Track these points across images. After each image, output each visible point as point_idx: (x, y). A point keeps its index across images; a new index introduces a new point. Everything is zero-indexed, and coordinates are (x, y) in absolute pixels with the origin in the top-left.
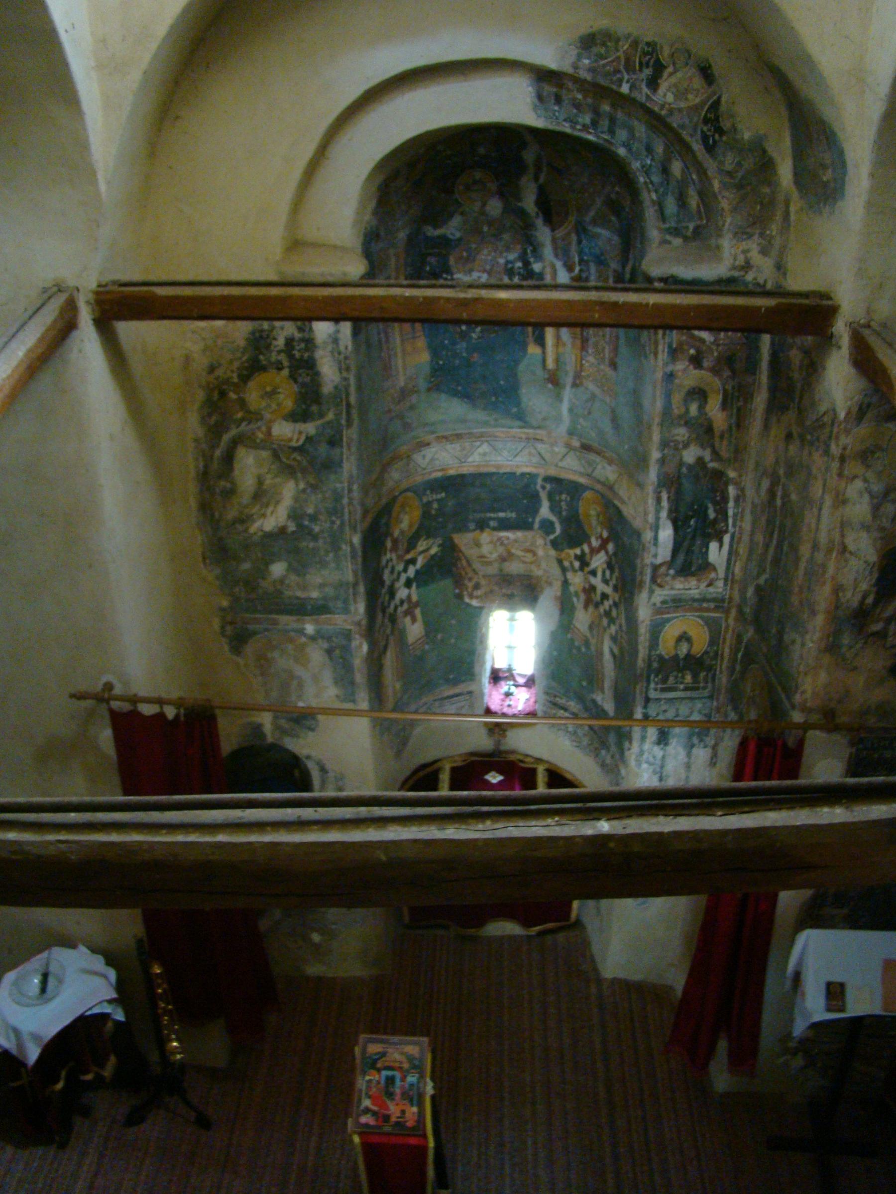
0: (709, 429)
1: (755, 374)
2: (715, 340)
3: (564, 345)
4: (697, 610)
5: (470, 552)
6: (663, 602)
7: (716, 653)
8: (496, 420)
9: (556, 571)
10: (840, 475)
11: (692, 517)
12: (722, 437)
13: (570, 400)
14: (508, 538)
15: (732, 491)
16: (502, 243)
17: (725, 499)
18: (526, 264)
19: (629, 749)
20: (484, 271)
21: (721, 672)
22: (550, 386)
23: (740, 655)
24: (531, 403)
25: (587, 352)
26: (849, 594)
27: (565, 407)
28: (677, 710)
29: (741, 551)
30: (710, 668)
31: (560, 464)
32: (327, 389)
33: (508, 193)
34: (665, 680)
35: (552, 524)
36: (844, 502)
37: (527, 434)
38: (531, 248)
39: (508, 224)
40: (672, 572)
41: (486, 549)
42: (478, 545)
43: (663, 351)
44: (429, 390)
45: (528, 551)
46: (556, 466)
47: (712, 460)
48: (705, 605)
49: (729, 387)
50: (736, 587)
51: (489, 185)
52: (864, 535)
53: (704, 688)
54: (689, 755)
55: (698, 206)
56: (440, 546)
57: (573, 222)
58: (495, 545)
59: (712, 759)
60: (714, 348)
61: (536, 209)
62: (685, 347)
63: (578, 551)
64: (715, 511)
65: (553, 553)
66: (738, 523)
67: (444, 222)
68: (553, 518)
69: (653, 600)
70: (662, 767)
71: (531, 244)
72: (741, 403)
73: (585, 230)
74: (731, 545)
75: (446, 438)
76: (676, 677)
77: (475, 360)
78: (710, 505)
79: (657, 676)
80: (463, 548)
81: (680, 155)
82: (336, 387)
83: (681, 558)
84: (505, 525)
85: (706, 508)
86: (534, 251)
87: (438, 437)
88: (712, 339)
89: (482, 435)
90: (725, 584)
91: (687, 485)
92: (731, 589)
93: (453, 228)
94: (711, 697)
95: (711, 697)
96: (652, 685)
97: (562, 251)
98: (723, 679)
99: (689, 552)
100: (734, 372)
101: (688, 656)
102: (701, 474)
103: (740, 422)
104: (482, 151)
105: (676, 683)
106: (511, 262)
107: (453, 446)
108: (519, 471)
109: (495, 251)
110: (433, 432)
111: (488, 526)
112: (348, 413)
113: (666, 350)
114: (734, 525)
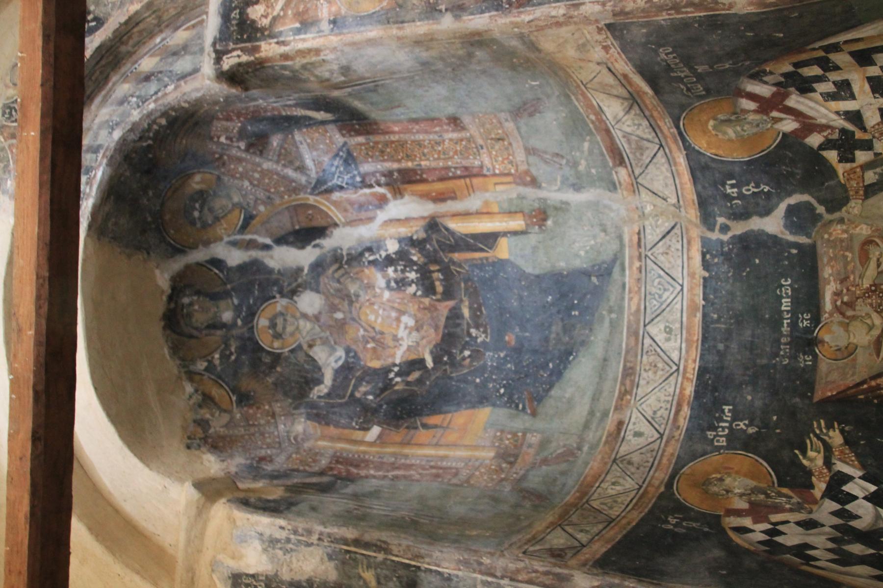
3: (486, 203)
5: (864, 364)
8: (610, 311)
13: (559, 190)
14: (837, 294)
16: (361, 293)
18: (389, 261)
20: (398, 320)
22: (549, 223)
24: (582, 253)
25: (481, 167)
31: (673, 200)
32: (330, 572)
33: (290, 284)
35: (791, 211)
37: (631, 258)
39: (337, 285)
41: (861, 337)
42: (850, 351)
43: (304, 40)
44: (534, 414)
45: (864, 258)
46: (678, 206)
51: (279, 308)
55: (187, 29)
56: (830, 426)
57: (318, 198)
58: (854, 318)
61: (309, 248)
63: (832, 156)
65: (855, 207)
67: (320, 369)
68: (783, 207)
71: (361, 254)
73: (320, 182)
75: (621, 397)
77: (513, 337)
80: (850, 381)
81: (136, 62)
82: (330, 557)
84: (809, 299)
86: (370, 249)
87: (616, 409)
89: (634, 333)
93: (329, 360)
97: (362, 213)
104: (227, 316)
106: (388, 283)
107: (642, 382)
108: (701, 273)
109: (373, 304)
110: (605, 414)
111: (809, 330)
112: (367, 545)
113: (302, 36)
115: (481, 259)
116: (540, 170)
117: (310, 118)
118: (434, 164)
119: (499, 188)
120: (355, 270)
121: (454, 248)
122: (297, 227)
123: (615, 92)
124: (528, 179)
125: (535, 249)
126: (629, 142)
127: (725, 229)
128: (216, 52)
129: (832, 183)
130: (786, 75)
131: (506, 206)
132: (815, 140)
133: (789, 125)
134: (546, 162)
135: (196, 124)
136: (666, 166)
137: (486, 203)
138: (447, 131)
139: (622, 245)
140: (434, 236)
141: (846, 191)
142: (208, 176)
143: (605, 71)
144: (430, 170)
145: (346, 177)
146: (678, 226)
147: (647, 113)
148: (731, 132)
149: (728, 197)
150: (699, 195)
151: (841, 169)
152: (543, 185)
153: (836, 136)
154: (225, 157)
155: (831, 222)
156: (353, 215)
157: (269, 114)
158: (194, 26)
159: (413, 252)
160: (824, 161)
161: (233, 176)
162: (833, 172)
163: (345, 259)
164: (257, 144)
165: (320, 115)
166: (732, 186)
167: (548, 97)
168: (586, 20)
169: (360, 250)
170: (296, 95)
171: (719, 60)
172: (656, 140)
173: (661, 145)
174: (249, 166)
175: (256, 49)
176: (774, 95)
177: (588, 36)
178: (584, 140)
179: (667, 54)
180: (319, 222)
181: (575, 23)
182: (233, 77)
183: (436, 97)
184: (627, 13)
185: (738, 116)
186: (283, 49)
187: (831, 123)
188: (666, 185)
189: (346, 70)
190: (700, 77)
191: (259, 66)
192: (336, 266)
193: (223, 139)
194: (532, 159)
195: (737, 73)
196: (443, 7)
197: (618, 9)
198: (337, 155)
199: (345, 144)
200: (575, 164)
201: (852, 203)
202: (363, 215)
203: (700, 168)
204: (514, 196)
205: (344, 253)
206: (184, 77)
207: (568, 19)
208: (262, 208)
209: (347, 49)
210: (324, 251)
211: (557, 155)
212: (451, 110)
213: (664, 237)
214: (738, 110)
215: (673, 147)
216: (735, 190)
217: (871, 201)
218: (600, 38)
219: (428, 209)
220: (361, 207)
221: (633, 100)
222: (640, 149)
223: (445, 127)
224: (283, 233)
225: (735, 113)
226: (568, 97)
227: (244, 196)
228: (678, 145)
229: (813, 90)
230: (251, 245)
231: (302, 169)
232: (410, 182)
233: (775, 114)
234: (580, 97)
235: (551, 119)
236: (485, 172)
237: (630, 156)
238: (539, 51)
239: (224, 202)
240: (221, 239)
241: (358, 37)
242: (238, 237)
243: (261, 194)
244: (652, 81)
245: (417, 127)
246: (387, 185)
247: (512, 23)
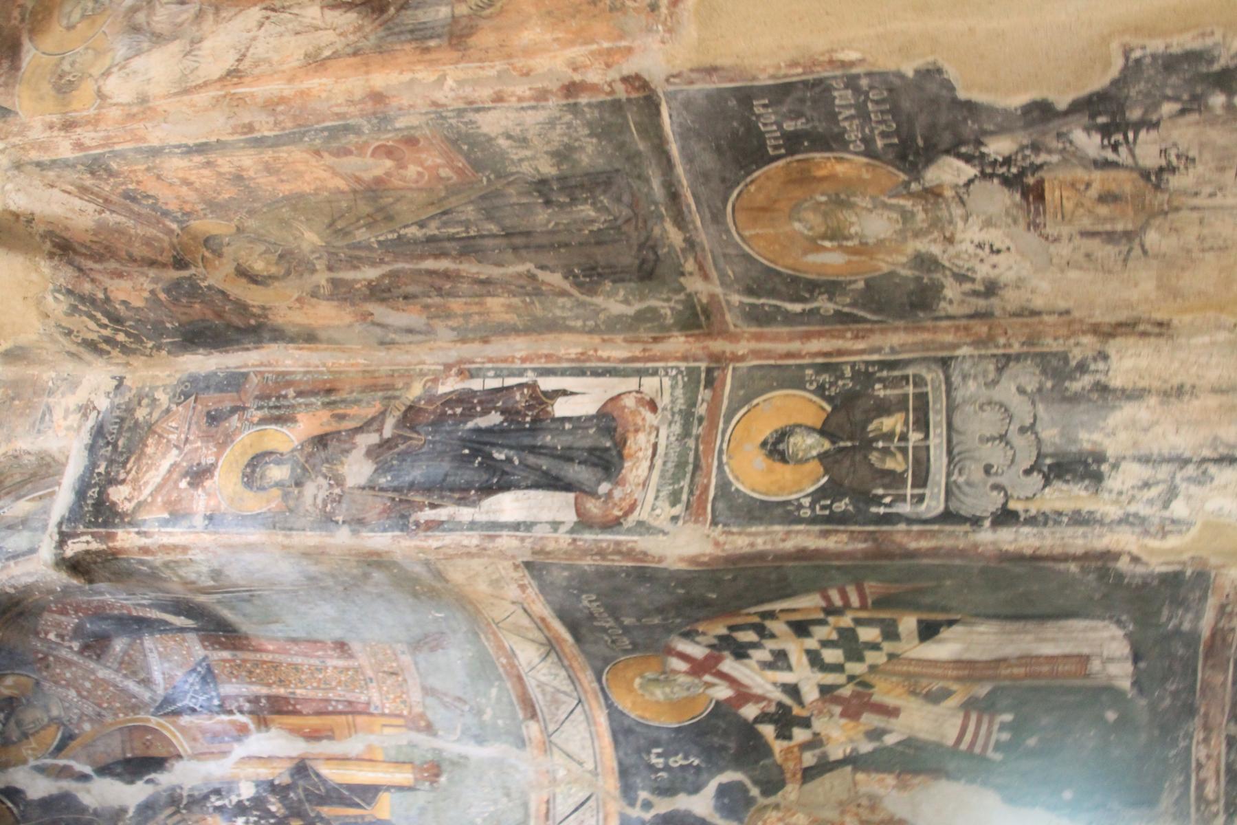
0: (321, 441)
1: (245, 376)
2: (177, 447)
3: (370, 748)
4: (713, 425)
6: (675, 499)
7: (825, 368)
9: (833, 785)
10: (94, 122)
11: (489, 457)
12: (342, 417)
13: (458, 740)
15: (450, 385)
17: (464, 399)
19: (1135, 559)
21: (878, 350)
22: (443, 779)
23: (797, 308)
25: (368, 704)
26: (328, 36)
27: (473, 751)
28: (985, 440)
29: (574, 352)
30: (865, 377)
31: (590, 765)
34: (894, 479)
35: (723, 791)
36: (143, 100)
38: (213, 798)
40: (604, 488)
43: (170, 534)
46: (595, 773)
47: (380, 430)
48: (701, 410)
49: (259, 414)
50: (658, 349)
52: (207, 44)
53: (919, 381)
54: (1135, 395)
55: (33, 499)
57: (161, 721)
59: (1144, 334)
60: (188, 447)
61: (140, 784)
62: (174, 496)
63: (768, 730)
64: (485, 412)
65: (791, 792)
66: (518, 365)
69: (662, 522)
70: (1184, 462)
71: (206, 797)
72: (291, 392)
73: (167, 701)
74: (563, 373)
76: (886, 452)
78: (470, 425)
79: (878, 500)
83: (576, 472)
85: (478, 430)
86: (217, 792)
88: (175, 452)
90: (655, 373)
91: (417, 473)
92: (661, 359)
94: (945, 363)
95: (945, 363)
96: (905, 508)
97: (215, 745)
98: (893, 340)
99: (567, 456)
100: (234, 410)
101: (823, 432)
102: (402, 447)
103: (326, 391)
105: (904, 451)
113: (169, 529)
114: (521, 373)
115: (355, 817)
116: (437, 714)
117: (166, 623)
118: (311, 694)
119: (387, 731)
120: (194, 818)
121: (323, 800)
122: (129, 755)
123: (530, 636)
124: (423, 724)
125: (423, 811)
126: (544, 693)
127: (647, 805)
128: (61, 533)
129: (767, 762)
130: (721, 638)
131: (392, 753)
132: (750, 711)
133: (723, 692)
134: (445, 706)
135: (21, 614)
136: (585, 724)
137: (370, 748)
138: (331, 657)
139: (527, 815)
140: (301, 783)
142: (23, 679)
143: (521, 611)
144: (306, 700)
145: (202, 698)
146: (593, 798)
148: (659, 693)
149: (652, 768)
150: (620, 764)
151: (778, 746)
152: (440, 733)
153: (772, 709)
154: (51, 659)
155: (766, 807)
156: (202, 746)
157: (116, 612)
158: (41, 497)
159: (272, 800)
160: (759, 736)
161: (56, 683)
162: (767, 751)
163: (185, 802)
164: (96, 645)
165: (180, 621)
166: (659, 755)
167: (454, 631)
168: (502, 555)
169: (206, 791)
170: (153, 595)
171: (648, 614)
172: (575, 694)
173: (580, 701)
174: (80, 673)
175: (111, 537)
176: (707, 658)
177: (503, 572)
178: (492, 686)
179: (590, 602)
180: (158, 751)
181: (489, 556)
182: (76, 566)
183: (323, 617)
184: (549, 553)
185: (667, 676)
186: (143, 541)
187: (768, 695)
188: (583, 748)
189: (216, 574)
190: (626, 630)
191: (112, 556)
192: (172, 809)
193: (52, 636)
194: (430, 701)
195: (668, 630)
196: (340, 519)
197: (537, 547)
198: (194, 670)
199: (206, 658)
200: (480, 713)
201: (789, 787)
202: (215, 748)
203: (622, 730)
204: (405, 742)
205: (185, 794)
206: (15, 556)
207: (481, 552)
208: (87, 727)
209: (220, 551)
210: (159, 788)
211: (459, 699)
212: (338, 633)
213: (576, 809)
214: (668, 670)
215: (594, 704)
216: (661, 760)
217: (809, 786)
218: (516, 575)
219: (298, 747)
220: (215, 736)
221: (551, 647)
222: (555, 702)
223: (330, 652)
224: (110, 761)
225: (664, 673)
226: (476, 634)
227: (66, 709)
228: (599, 702)
229: (747, 656)
230: (64, 773)
231: (146, 682)
232: (280, 712)
233: (707, 678)
234: (491, 637)
235: (455, 658)
236: (372, 710)
237: (545, 709)
238: (447, 581)
239: (39, 714)
240: (25, 762)
241: (236, 540)
242: (49, 761)
243: (89, 709)
244: (574, 628)
245: (296, 648)
246: (251, 713)
247: (417, 547)
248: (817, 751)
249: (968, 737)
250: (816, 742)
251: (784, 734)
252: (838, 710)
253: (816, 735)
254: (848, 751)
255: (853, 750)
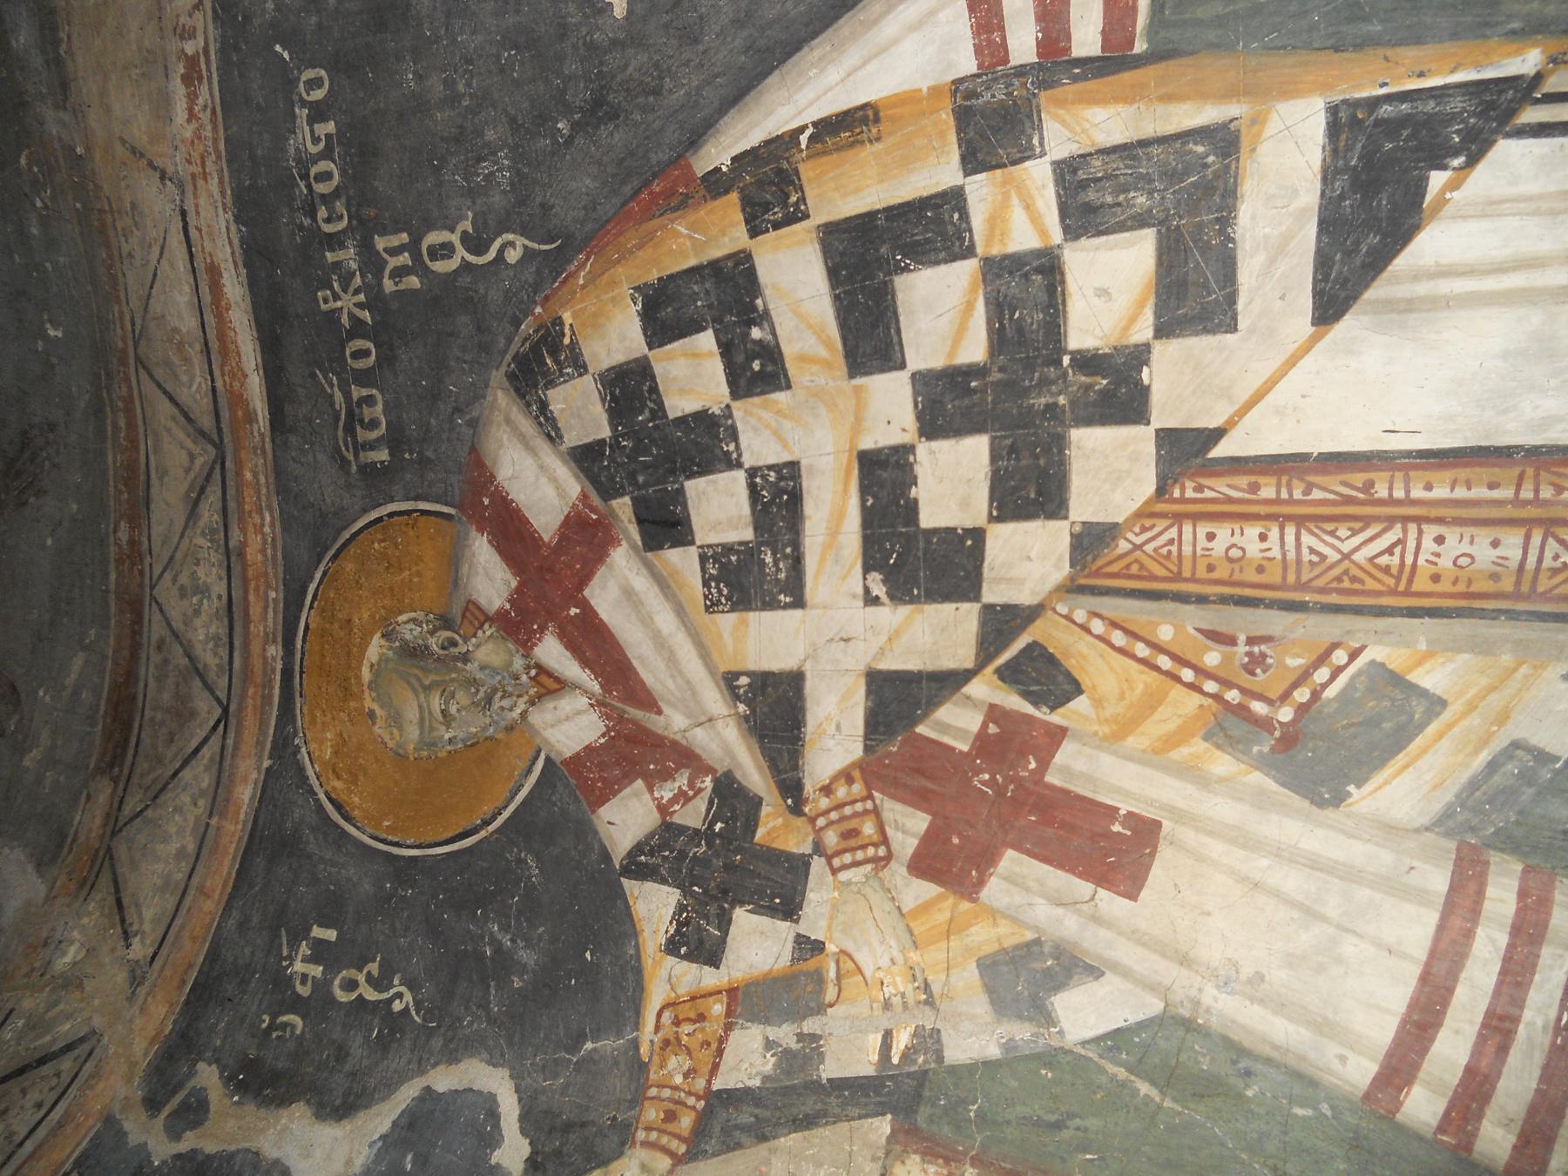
63: (655, 906)
133: (571, 726)
141: (638, 1099)
147: (236, 536)
166: (321, 953)
225: (446, 622)
228: (263, 724)
248: (785, 1034)
249: (1452, 1048)
250: (796, 990)
251: (698, 941)
252: (908, 826)
253: (808, 947)
254: (902, 1040)
255: (928, 1040)
